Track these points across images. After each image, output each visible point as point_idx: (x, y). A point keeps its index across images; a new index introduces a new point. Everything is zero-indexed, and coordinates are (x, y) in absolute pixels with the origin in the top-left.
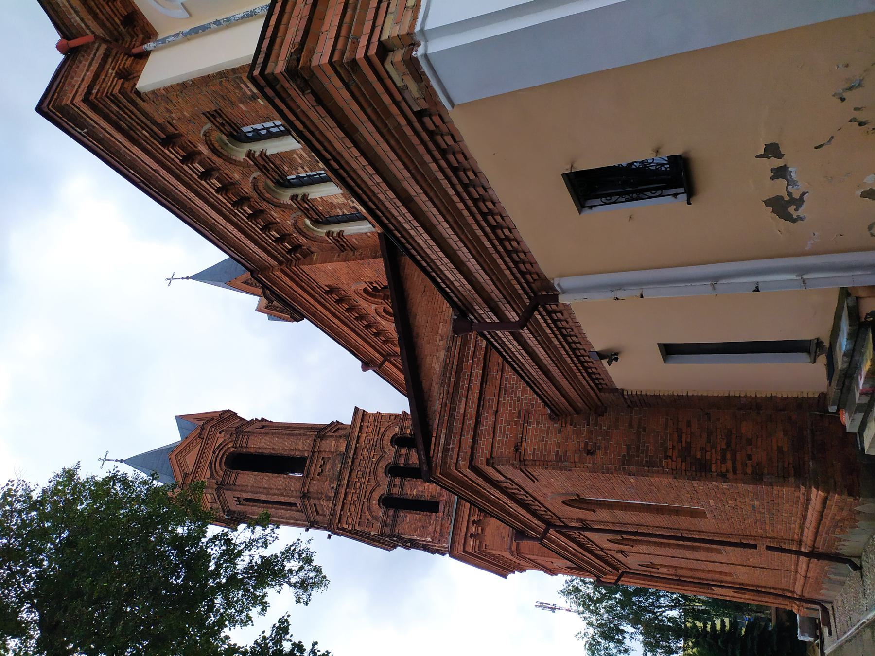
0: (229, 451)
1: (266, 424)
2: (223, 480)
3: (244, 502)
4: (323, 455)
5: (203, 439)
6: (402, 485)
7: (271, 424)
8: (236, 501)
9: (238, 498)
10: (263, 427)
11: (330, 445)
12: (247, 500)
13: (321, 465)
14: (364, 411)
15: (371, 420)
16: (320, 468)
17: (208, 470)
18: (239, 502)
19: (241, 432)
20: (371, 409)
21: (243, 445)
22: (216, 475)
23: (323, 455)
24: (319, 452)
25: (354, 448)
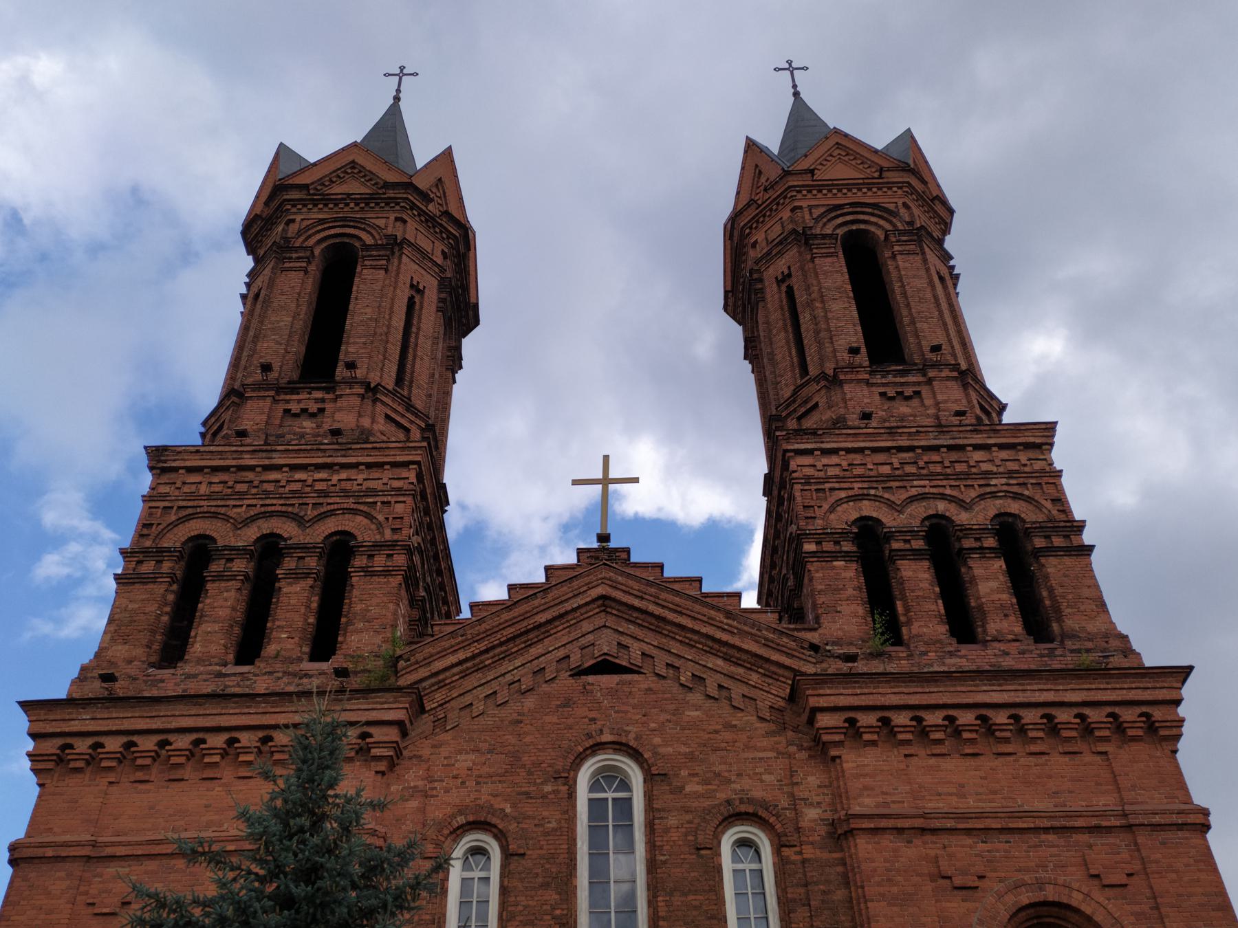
0: (872, 229)
1: (949, 283)
2: (815, 236)
3: (784, 288)
4: (925, 391)
5: (880, 177)
6: (916, 554)
7: (953, 296)
8: (783, 272)
9: (789, 275)
10: (941, 279)
11: (951, 395)
12: (790, 293)
13: (902, 393)
14: (1052, 445)
15: (1038, 465)
16: (897, 392)
17: (822, 210)
18: (783, 281)
19: (920, 241)
20: (1059, 456)
21: (896, 248)
22: (821, 224)
23: (925, 391)
24: (930, 382)
25: (961, 442)
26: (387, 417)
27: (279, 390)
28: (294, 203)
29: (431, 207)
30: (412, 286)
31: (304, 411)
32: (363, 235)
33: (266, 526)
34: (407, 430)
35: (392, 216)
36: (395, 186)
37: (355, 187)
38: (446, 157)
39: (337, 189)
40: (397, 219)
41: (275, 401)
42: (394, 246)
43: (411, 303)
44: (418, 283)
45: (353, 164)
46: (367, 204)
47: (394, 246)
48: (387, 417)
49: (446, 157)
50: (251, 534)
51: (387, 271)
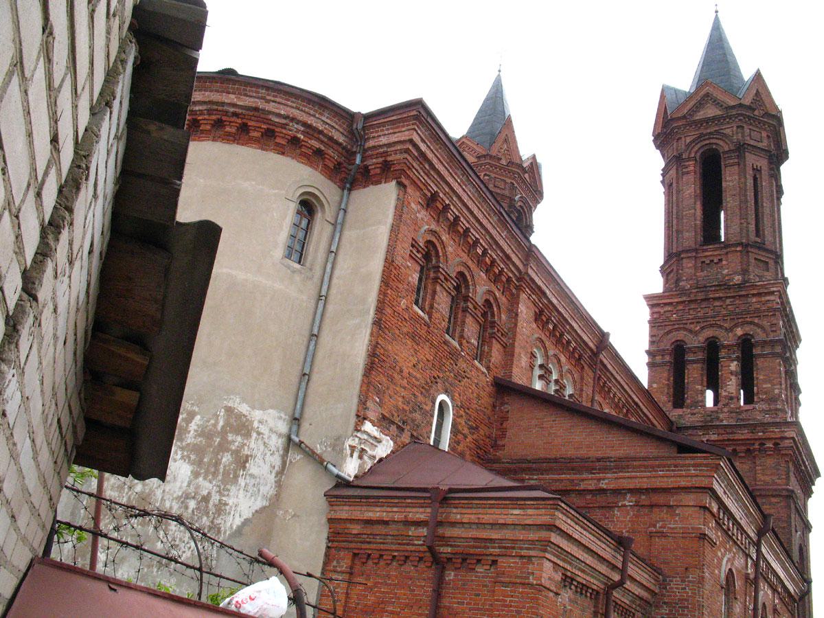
26: (756, 259)
27: (696, 250)
28: (679, 127)
29: (756, 113)
30: (754, 169)
31: (712, 261)
32: (721, 143)
33: (709, 333)
34: (767, 263)
35: (735, 125)
36: (733, 107)
37: (710, 111)
38: (758, 77)
39: (700, 115)
40: (738, 127)
41: (696, 257)
42: (741, 149)
43: (755, 179)
44: (757, 166)
45: (707, 95)
46: (719, 121)
47: (741, 149)
48: (756, 259)
49: (758, 77)
50: (702, 338)
51: (739, 165)
